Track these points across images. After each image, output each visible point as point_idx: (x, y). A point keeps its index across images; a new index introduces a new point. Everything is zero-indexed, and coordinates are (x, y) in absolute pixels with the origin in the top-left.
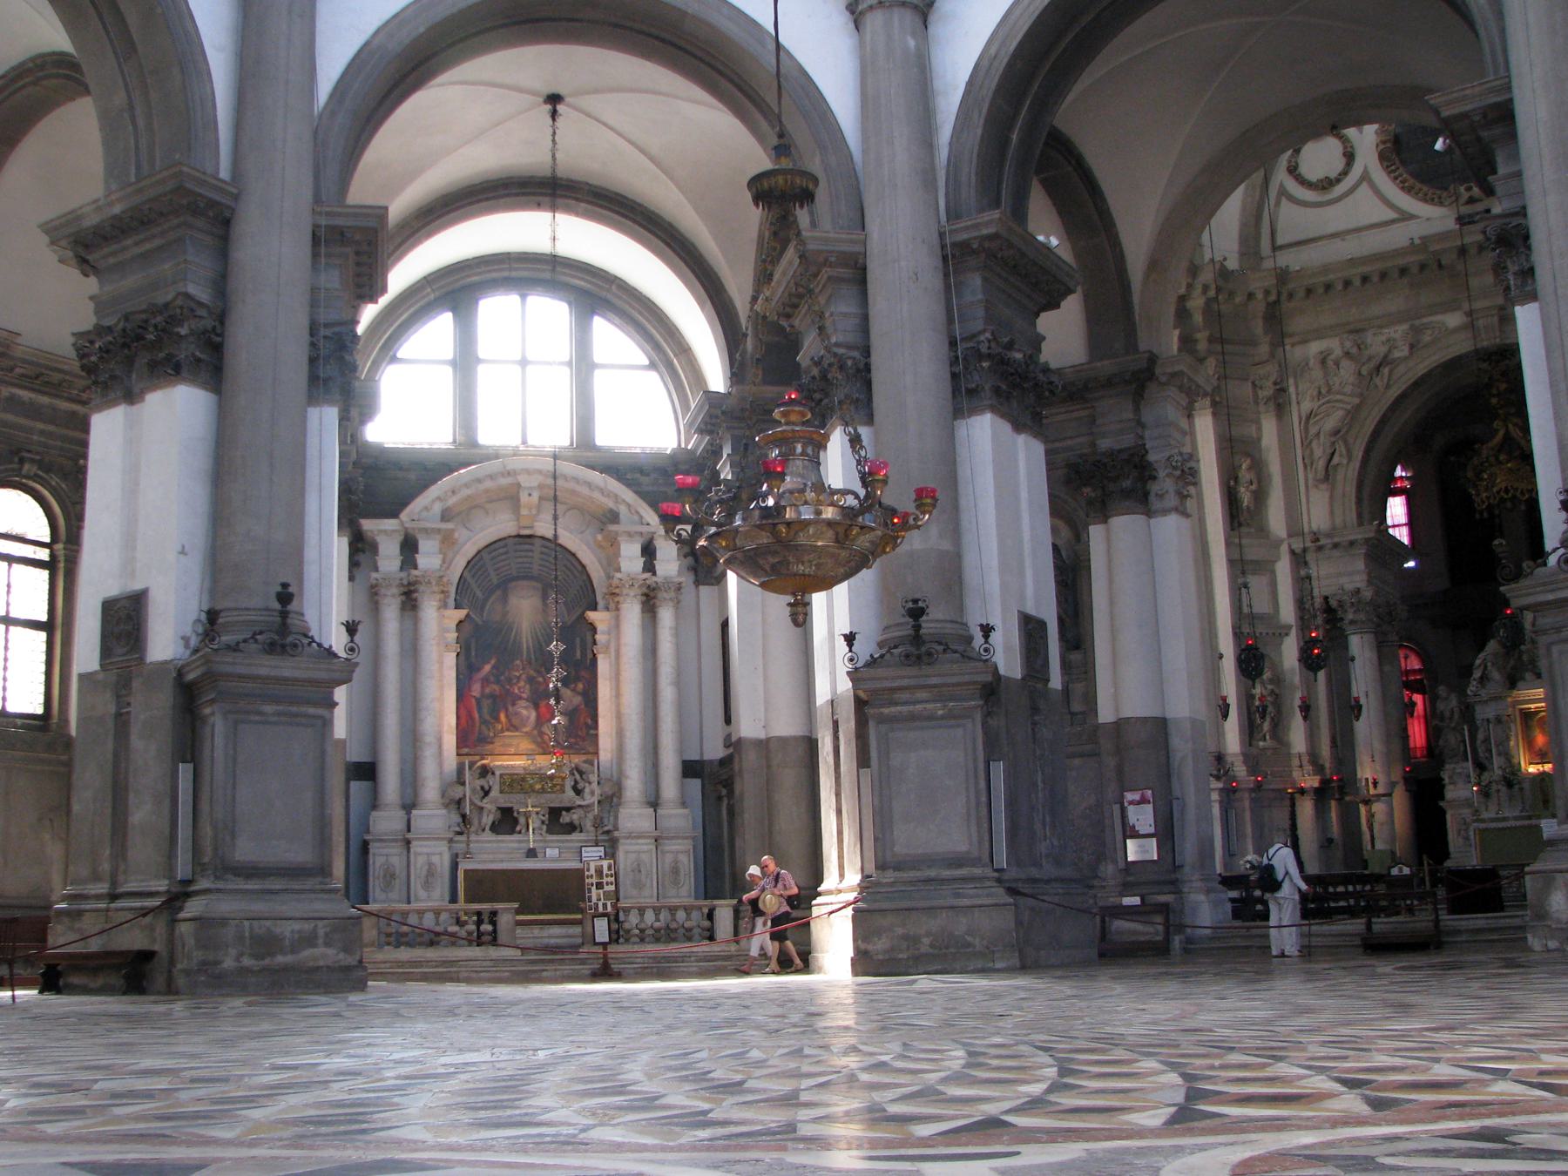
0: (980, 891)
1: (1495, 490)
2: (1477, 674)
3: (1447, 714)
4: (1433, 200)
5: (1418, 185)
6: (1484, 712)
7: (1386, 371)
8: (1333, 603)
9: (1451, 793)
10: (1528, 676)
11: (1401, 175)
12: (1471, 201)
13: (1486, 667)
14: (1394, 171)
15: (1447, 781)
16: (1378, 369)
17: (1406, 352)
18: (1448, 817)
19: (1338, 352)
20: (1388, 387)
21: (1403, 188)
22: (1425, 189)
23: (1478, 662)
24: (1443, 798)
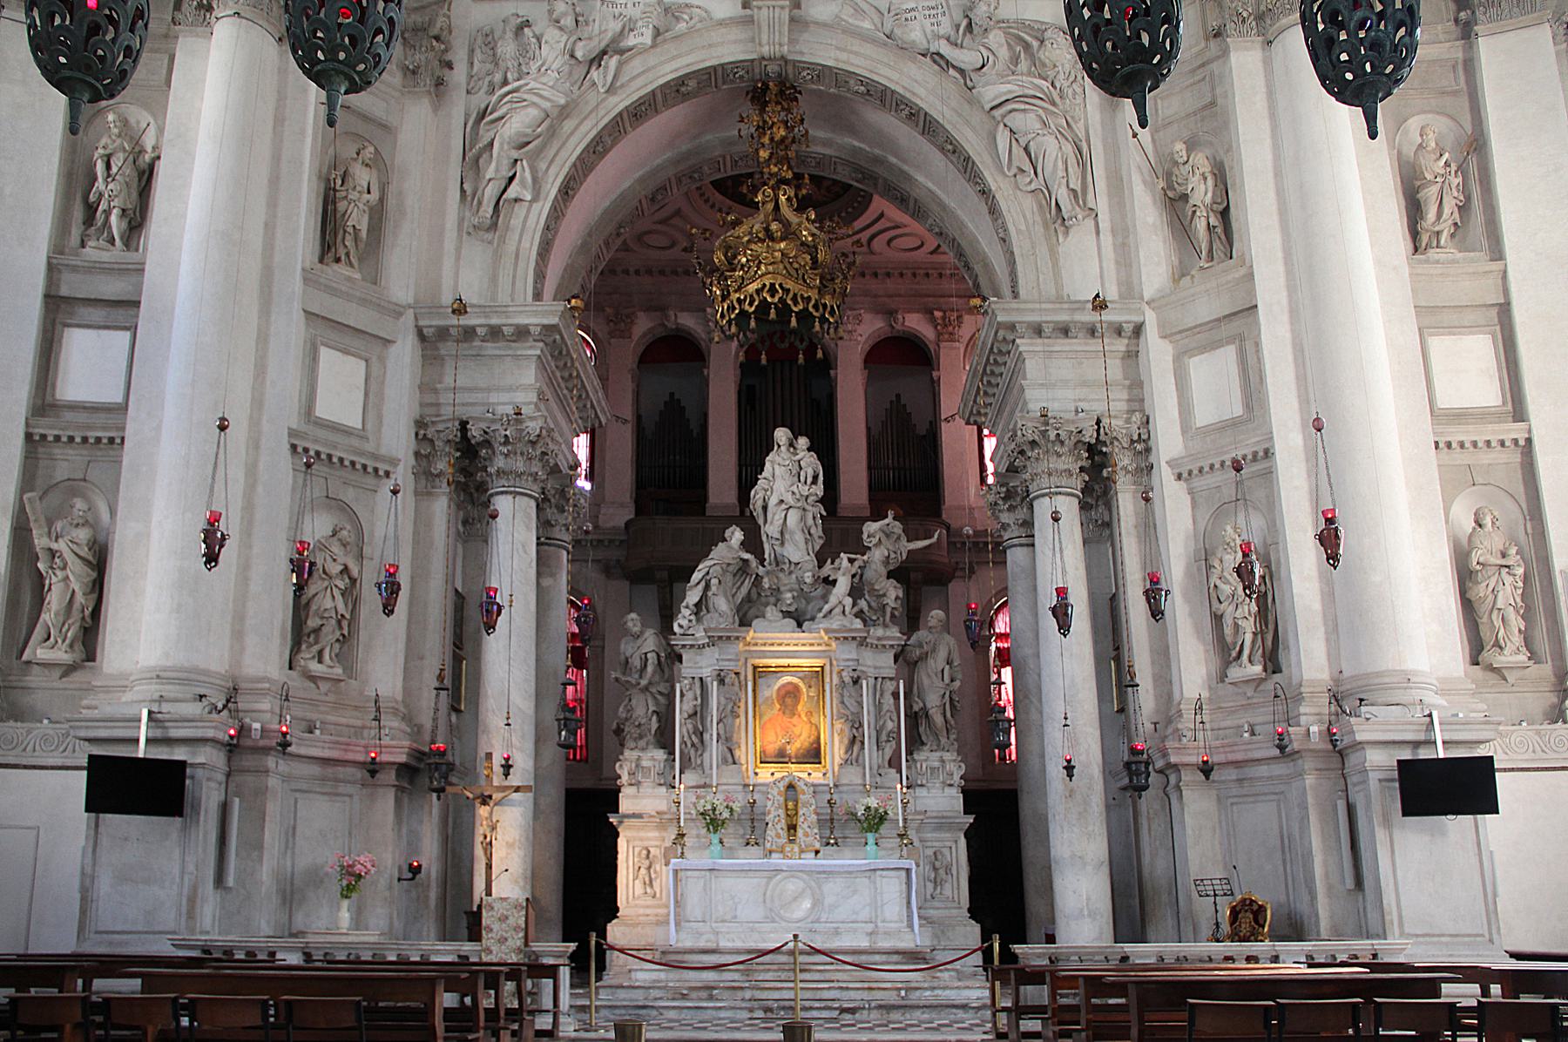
2: (693, 597)
3: (636, 662)
6: (699, 664)
15: (625, 778)
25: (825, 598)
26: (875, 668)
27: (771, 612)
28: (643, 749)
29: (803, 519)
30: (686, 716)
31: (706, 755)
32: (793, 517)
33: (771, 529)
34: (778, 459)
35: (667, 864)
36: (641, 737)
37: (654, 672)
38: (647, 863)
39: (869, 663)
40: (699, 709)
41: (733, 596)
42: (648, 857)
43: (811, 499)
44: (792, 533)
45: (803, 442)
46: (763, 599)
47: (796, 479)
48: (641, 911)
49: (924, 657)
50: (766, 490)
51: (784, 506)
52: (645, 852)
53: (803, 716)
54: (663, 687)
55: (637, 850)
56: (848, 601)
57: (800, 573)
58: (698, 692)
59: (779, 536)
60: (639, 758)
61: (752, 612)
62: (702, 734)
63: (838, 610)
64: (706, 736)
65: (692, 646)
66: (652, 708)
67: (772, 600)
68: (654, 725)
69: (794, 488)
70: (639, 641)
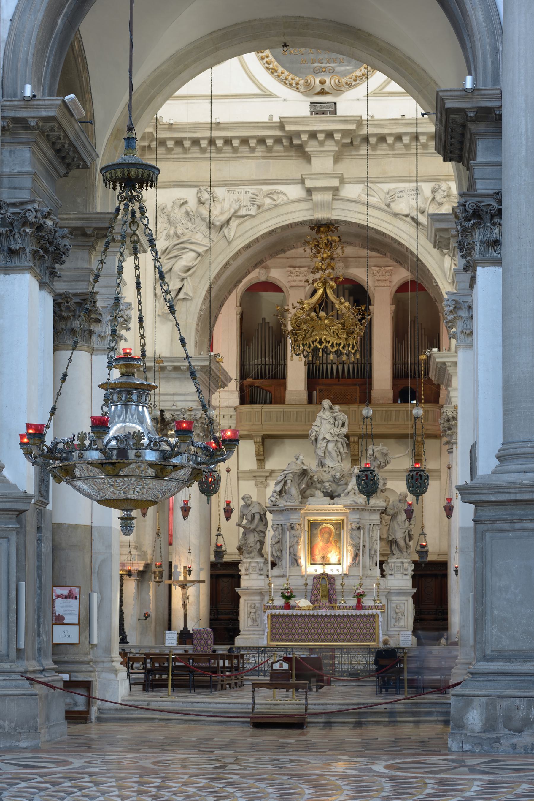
0: (8, 683)
3: (249, 518)
8: (168, 416)
9: (244, 583)
10: (319, 493)
13: (285, 483)
15: (242, 572)
26: (370, 520)
28: (253, 558)
30: (274, 543)
31: (284, 562)
37: (259, 522)
39: (367, 518)
44: (330, 453)
46: (314, 485)
53: (333, 542)
57: (333, 473)
58: (281, 531)
61: (308, 492)
62: (282, 551)
65: (277, 510)
66: (256, 539)
70: (250, 508)
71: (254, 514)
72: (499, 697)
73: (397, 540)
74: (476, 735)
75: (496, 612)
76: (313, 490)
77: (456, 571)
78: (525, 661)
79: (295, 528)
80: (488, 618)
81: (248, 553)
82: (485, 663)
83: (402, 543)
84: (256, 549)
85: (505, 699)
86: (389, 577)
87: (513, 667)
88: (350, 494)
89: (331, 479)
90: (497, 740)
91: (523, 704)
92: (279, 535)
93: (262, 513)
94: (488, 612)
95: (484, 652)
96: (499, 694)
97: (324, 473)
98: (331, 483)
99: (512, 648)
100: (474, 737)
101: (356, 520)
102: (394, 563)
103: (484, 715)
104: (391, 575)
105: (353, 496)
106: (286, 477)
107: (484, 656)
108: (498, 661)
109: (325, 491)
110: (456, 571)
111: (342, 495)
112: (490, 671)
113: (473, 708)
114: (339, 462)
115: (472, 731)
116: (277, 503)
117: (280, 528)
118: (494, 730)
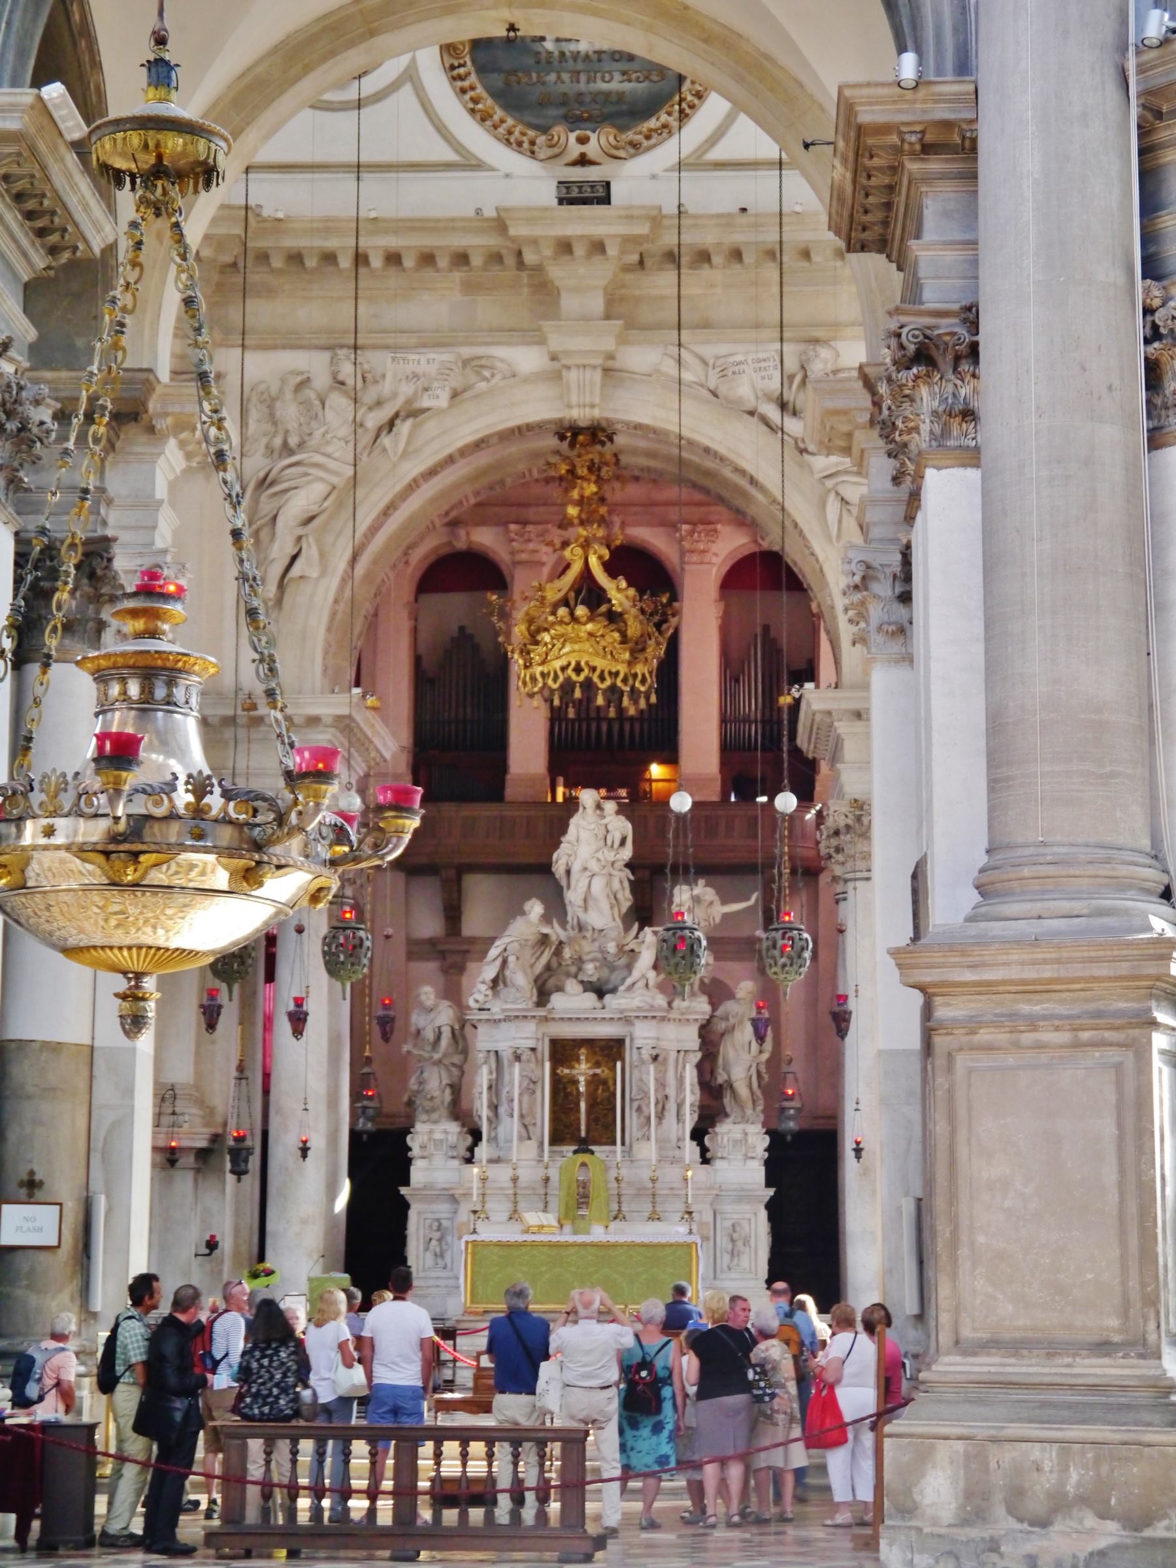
1: (557, 664)
3: (430, 1035)
4: (520, 144)
5: (499, 113)
7: (404, 428)
9: (419, 1173)
11: (472, 88)
12: (583, 161)
13: (505, 962)
14: (461, 78)
15: (415, 1152)
16: (391, 425)
17: (443, 401)
18: (412, 1215)
19: (321, 380)
20: (405, 455)
21: (472, 111)
22: (510, 121)
23: (493, 952)
24: (407, 1183)
25: (629, 967)
26: (679, 1041)
27: (572, 986)
28: (436, 1122)
29: (609, 884)
32: (598, 885)
33: (573, 897)
34: (583, 823)
35: (460, 1238)
36: (433, 1110)
38: (437, 1235)
40: (494, 1083)
41: (532, 966)
42: (439, 1229)
43: (620, 864)
45: (610, 806)
46: (564, 968)
47: (602, 842)
48: (431, 1283)
49: (731, 1030)
50: (570, 856)
51: (588, 874)
52: (436, 1224)
54: (457, 1059)
55: (428, 1222)
56: (652, 974)
58: (494, 1066)
59: (581, 903)
60: (431, 1132)
62: (496, 1107)
63: (641, 984)
64: (502, 1110)
65: (488, 1020)
66: (446, 1081)
67: (573, 969)
68: (448, 1096)
69: (600, 855)
70: (432, 1015)
71: (439, 1028)
72: (994, 1440)
73: (736, 1085)
74: (943, 1531)
75: (981, 1239)
76: (563, 978)
77: (858, 1151)
78: (1049, 1355)
79: (523, 1058)
80: (963, 1251)
81: (427, 1112)
82: (958, 1359)
83: (743, 1091)
84: (442, 1102)
85: (1007, 1446)
86: (718, 1164)
87: (1024, 1370)
88: (637, 986)
89: (599, 955)
90: (993, 1546)
91: (1048, 1457)
92: (491, 1073)
93: (457, 1027)
94: (964, 1238)
95: (957, 1332)
96: (993, 1432)
97: (584, 943)
98: (598, 964)
99: (1021, 1323)
100: (940, 1536)
101: (649, 1041)
102: (728, 1133)
103: (961, 1485)
104: (722, 1158)
105: (644, 991)
106: (505, 950)
107: (957, 1342)
108: (988, 1355)
109: (586, 979)
110: (858, 1151)
111: (622, 988)
112: (972, 1377)
113: (934, 1467)
114: (614, 920)
115: (935, 1522)
116: (486, 1006)
117: (492, 1055)
118: (984, 1520)
